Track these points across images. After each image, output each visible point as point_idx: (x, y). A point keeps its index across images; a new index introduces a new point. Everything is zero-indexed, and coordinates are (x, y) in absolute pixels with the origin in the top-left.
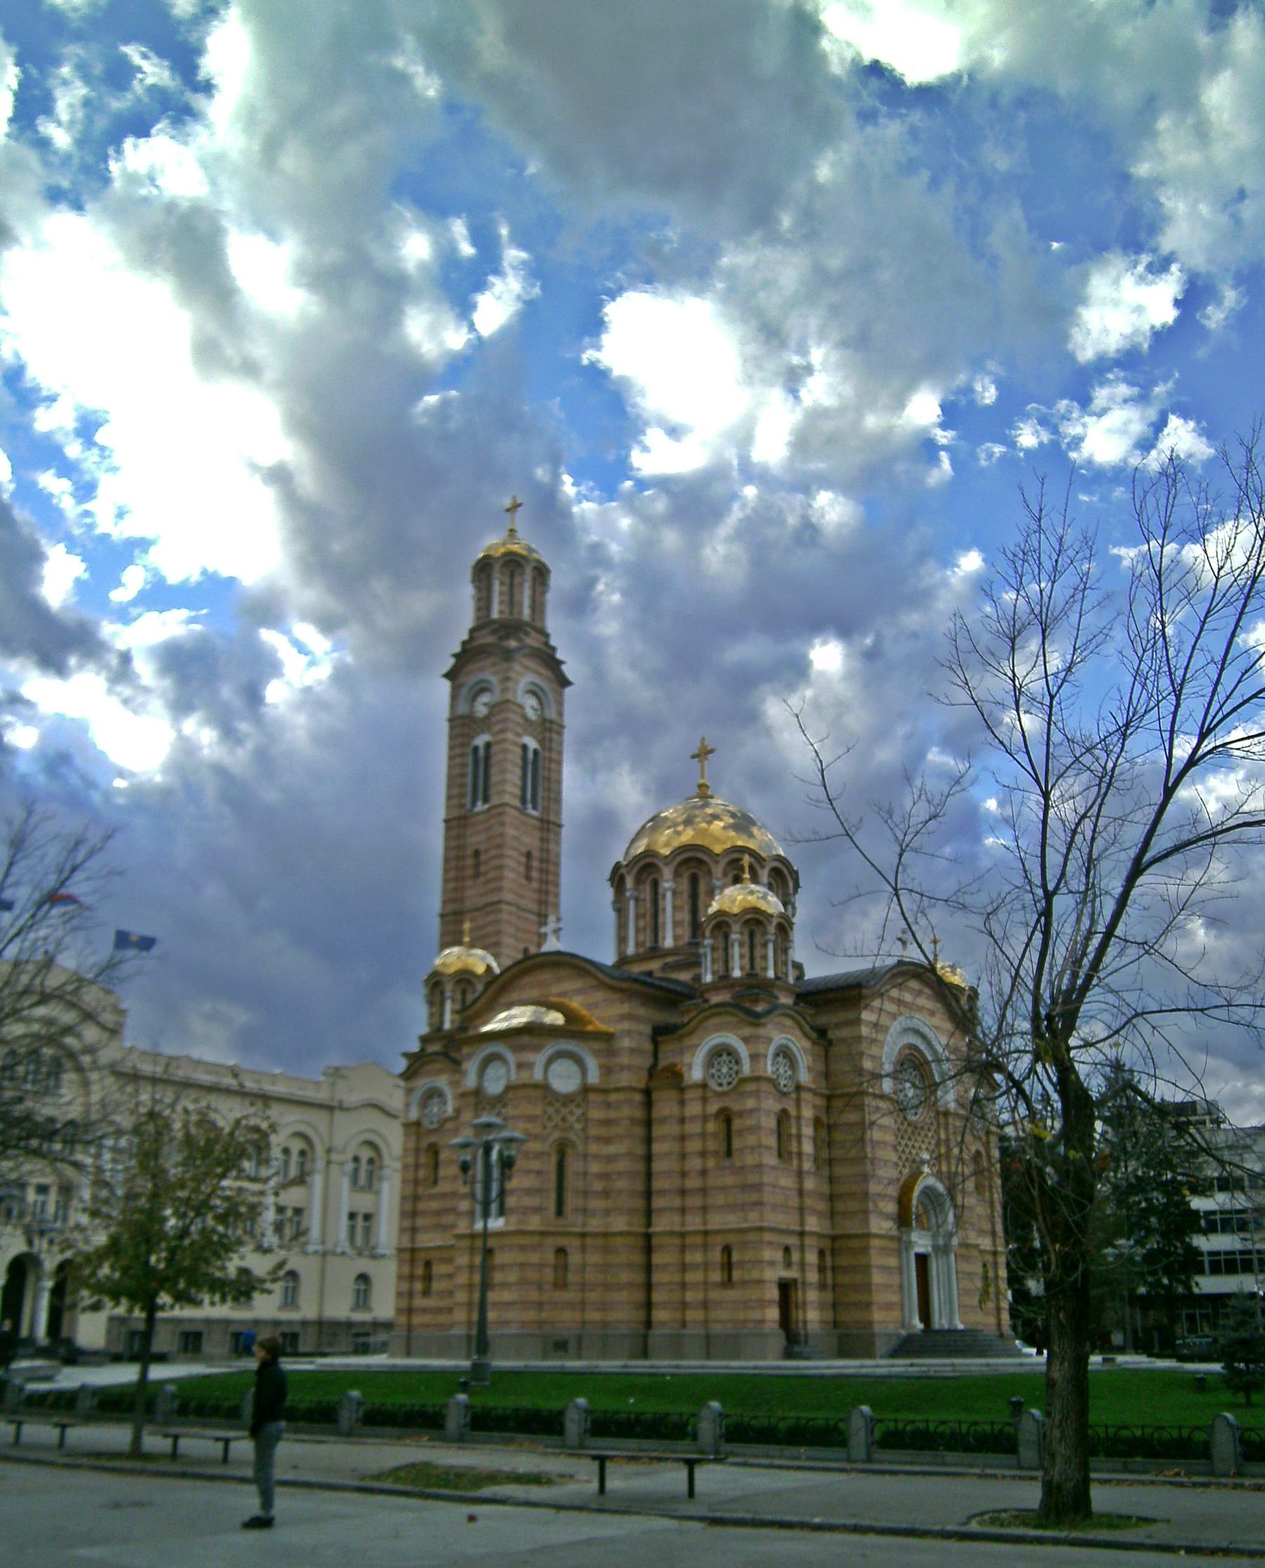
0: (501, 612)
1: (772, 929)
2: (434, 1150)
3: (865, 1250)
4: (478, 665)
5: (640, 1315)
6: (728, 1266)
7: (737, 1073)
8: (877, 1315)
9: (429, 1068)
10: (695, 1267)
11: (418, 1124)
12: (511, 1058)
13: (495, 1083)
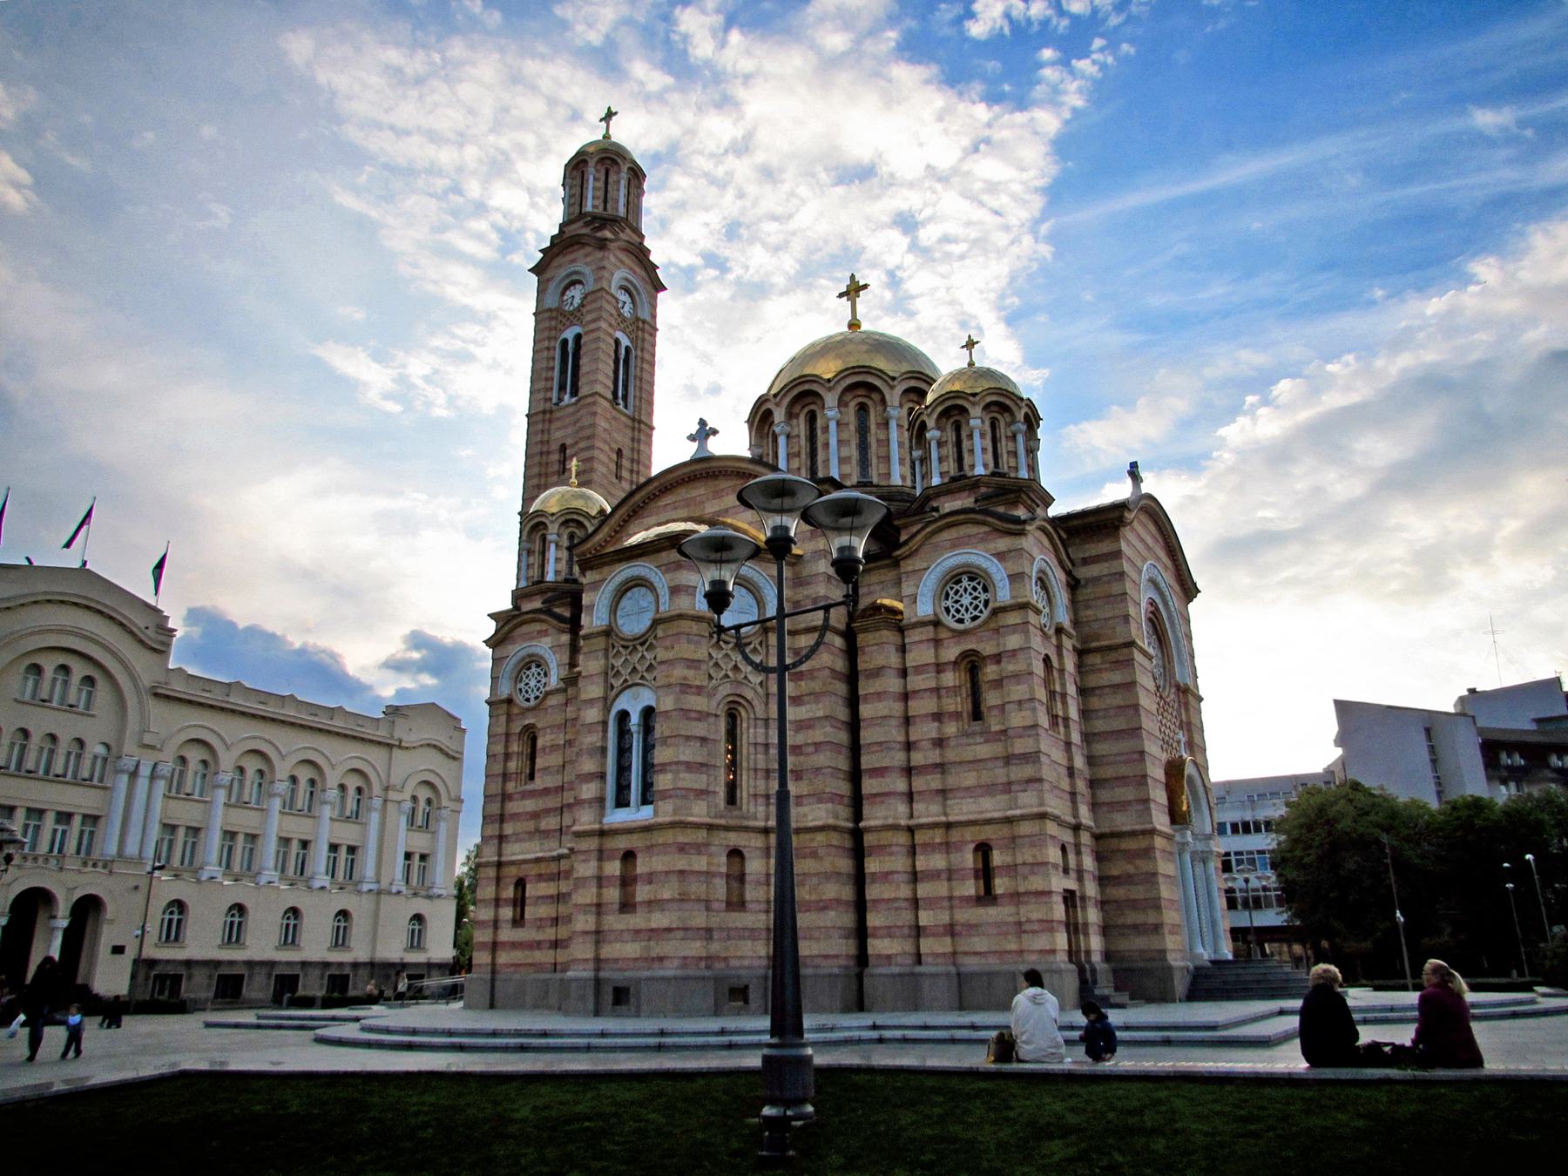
0: (594, 207)
1: (1020, 416)
2: (531, 735)
3: (1148, 853)
4: (570, 257)
5: (847, 947)
6: (985, 873)
7: (986, 603)
8: (1171, 942)
9: (525, 629)
10: (934, 875)
11: (509, 701)
12: (661, 581)
13: (633, 623)
